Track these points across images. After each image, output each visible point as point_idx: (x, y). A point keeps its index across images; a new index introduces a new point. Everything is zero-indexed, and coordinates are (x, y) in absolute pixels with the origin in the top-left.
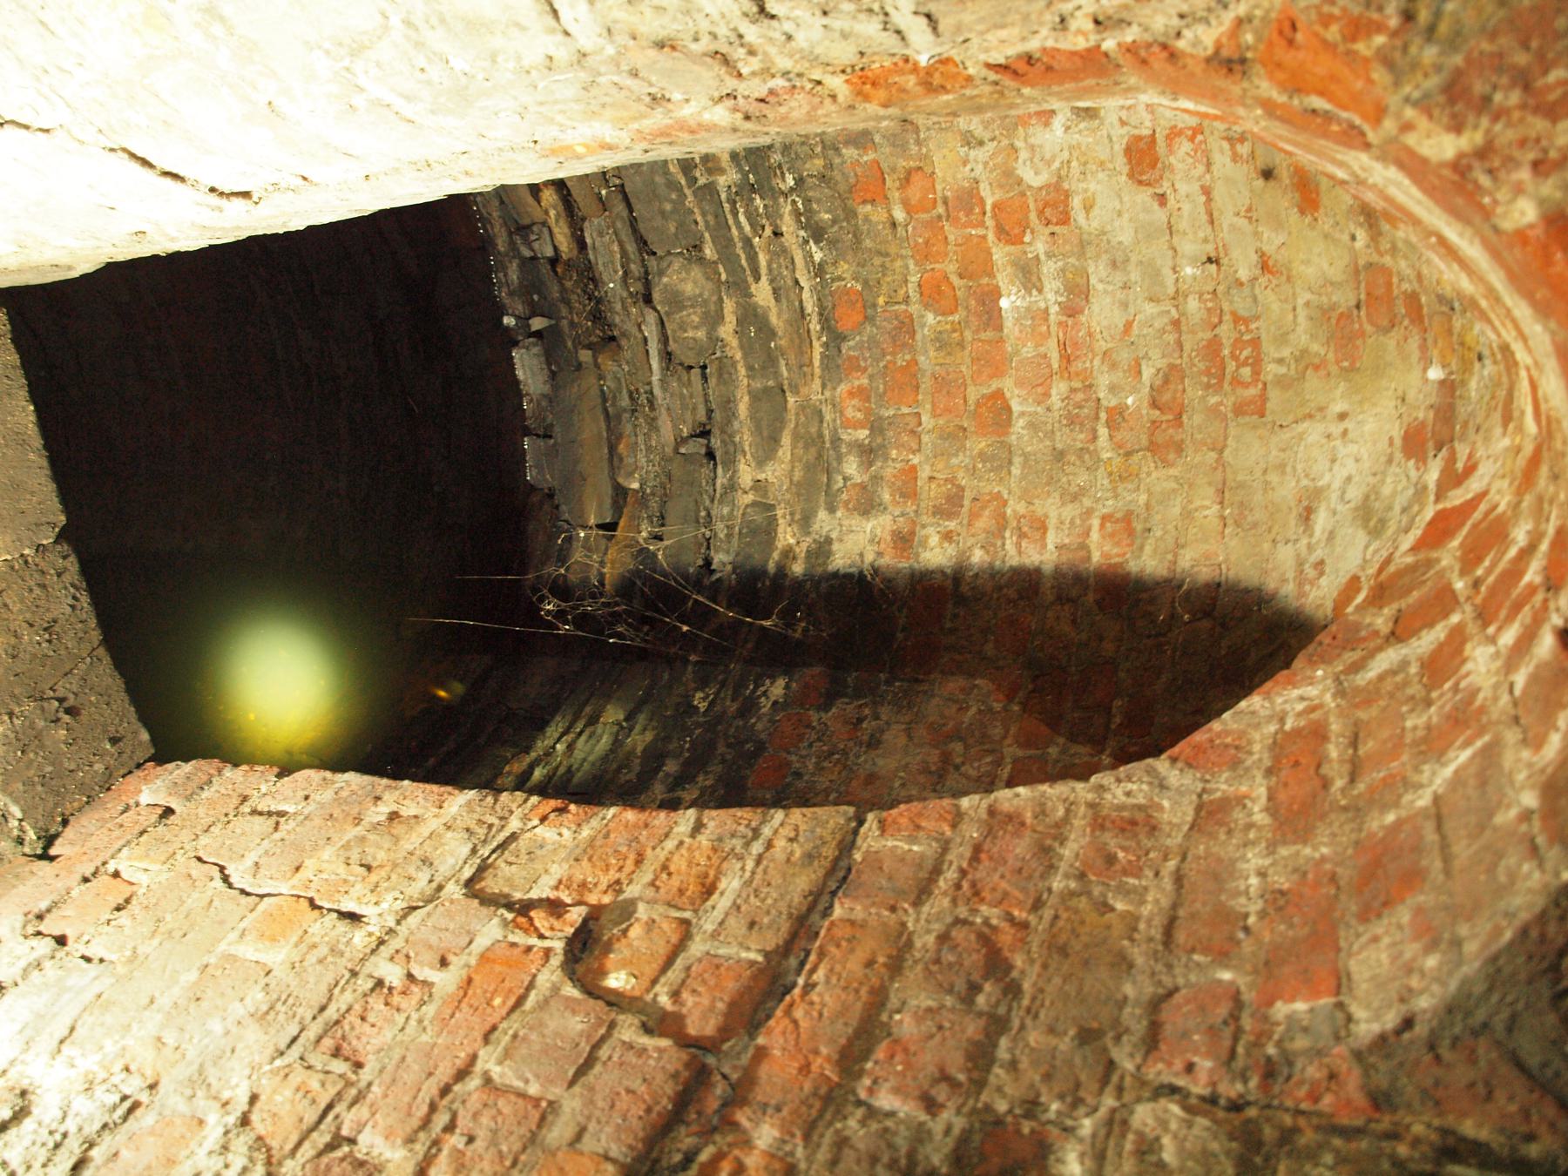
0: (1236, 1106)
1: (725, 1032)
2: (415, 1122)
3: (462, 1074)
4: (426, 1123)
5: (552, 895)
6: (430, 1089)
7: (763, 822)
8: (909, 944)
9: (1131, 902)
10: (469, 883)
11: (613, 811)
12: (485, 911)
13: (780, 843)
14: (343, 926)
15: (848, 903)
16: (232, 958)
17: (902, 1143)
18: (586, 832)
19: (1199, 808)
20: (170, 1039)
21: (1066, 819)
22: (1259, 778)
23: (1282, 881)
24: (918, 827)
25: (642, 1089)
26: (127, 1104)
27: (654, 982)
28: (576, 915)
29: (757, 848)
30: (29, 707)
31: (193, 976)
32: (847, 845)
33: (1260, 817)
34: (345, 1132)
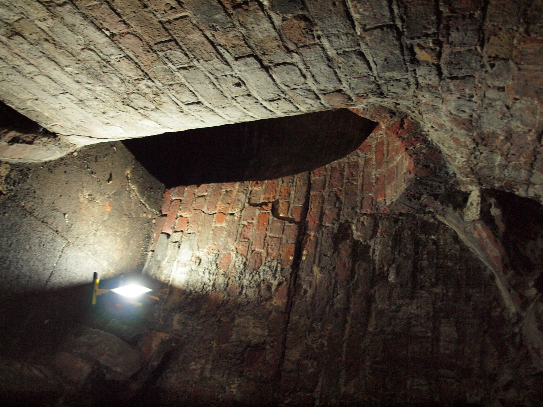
0: (374, 214)
1: (301, 219)
2: (263, 246)
3: (266, 236)
4: (264, 245)
5: (264, 201)
6: (262, 240)
7: (294, 178)
8: (324, 198)
9: (356, 182)
10: (249, 202)
11: (266, 181)
12: (255, 208)
13: (298, 182)
14: (232, 217)
15: (313, 192)
16: (216, 227)
17: (331, 230)
18: (264, 187)
19: (365, 160)
20: (216, 243)
21: (344, 167)
22: (374, 155)
23: (378, 176)
24: (320, 173)
25: (293, 232)
26: (217, 255)
27: (287, 214)
28: (270, 205)
29: (294, 184)
30: (146, 192)
31: (212, 232)
32: (309, 179)
33: (374, 163)
34: (253, 249)
